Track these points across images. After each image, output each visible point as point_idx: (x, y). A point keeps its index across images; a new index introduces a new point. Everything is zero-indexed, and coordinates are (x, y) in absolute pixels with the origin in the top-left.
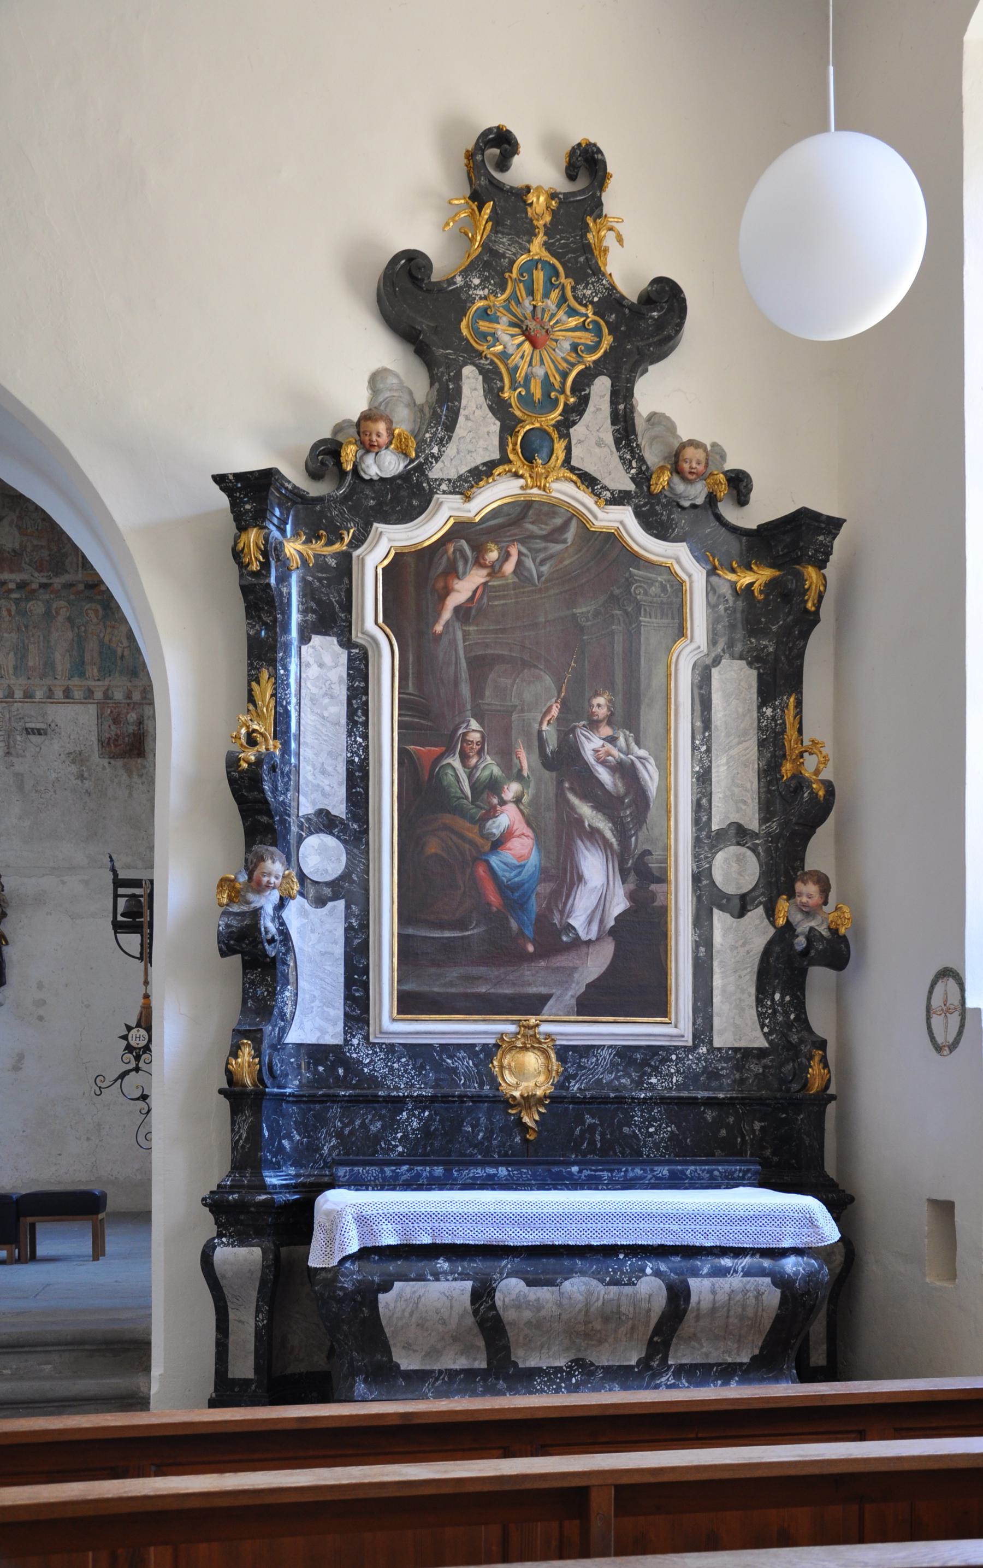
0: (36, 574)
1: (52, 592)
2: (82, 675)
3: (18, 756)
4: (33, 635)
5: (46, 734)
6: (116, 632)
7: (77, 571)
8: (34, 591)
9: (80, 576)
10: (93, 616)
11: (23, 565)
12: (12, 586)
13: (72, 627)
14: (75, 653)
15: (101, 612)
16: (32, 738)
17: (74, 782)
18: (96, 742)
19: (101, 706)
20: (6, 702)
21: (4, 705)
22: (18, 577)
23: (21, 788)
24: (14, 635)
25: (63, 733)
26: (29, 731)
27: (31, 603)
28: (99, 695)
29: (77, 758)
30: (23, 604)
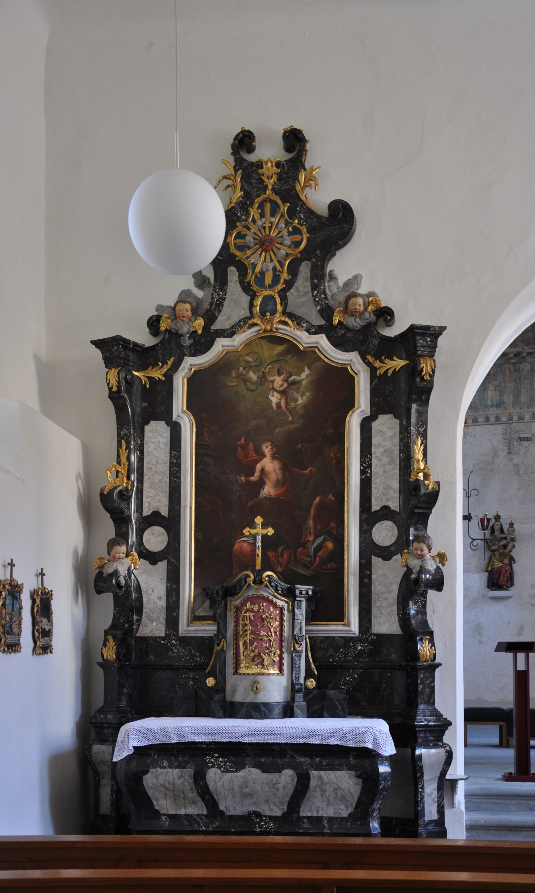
0: (525, 347)
3: (515, 454)
5: (531, 440)
8: (524, 357)
12: (511, 355)
20: (508, 423)
21: (507, 425)
23: (518, 472)
24: (513, 384)
26: (521, 439)
27: (523, 364)
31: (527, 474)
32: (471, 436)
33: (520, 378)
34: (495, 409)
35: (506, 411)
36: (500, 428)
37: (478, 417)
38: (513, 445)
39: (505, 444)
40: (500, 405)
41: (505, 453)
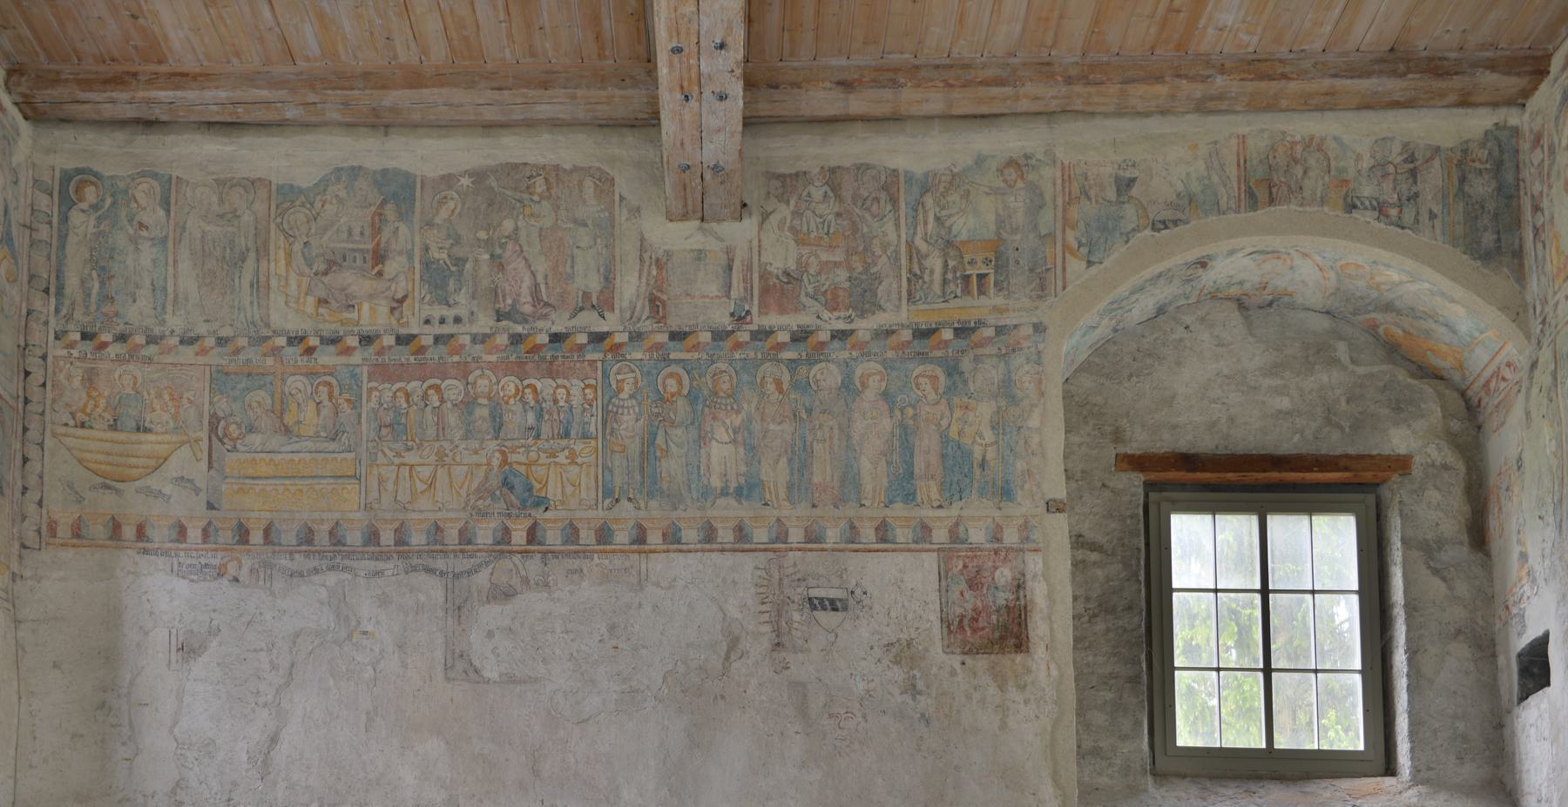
0: (826, 315)
1: (853, 347)
2: (910, 497)
4: (821, 426)
5: (845, 609)
6: (971, 417)
7: (898, 307)
8: (823, 344)
9: (904, 316)
10: (929, 388)
11: (803, 299)
12: (783, 337)
13: (891, 411)
14: (896, 457)
15: (942, 378)
16: (821, 615)
17: (900, 699)
18: (937, 624)
19: (946, 555)
21: (771, 555)
22: (794, 321)
23: (803, 711)
24: (788, 427)
25: (877, 607)
26: (815, 604)
28: (940, 535)
29: (904, 653)
30: (803, 370)
31: (831, 716)
32: (658, 585)
33: (809, 411)
34: (732, 502)
35: (767, 511)
36: (747, 567)
37: (682, 525)
38: (790, 622)
39: (766, 617)
40: (747, 490)
41: (766, 643)
